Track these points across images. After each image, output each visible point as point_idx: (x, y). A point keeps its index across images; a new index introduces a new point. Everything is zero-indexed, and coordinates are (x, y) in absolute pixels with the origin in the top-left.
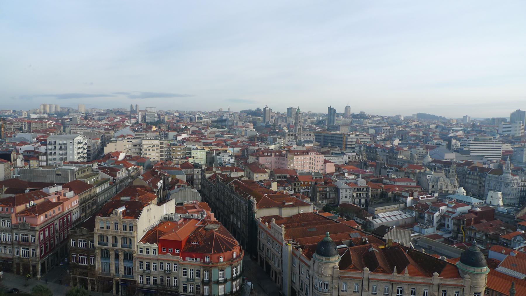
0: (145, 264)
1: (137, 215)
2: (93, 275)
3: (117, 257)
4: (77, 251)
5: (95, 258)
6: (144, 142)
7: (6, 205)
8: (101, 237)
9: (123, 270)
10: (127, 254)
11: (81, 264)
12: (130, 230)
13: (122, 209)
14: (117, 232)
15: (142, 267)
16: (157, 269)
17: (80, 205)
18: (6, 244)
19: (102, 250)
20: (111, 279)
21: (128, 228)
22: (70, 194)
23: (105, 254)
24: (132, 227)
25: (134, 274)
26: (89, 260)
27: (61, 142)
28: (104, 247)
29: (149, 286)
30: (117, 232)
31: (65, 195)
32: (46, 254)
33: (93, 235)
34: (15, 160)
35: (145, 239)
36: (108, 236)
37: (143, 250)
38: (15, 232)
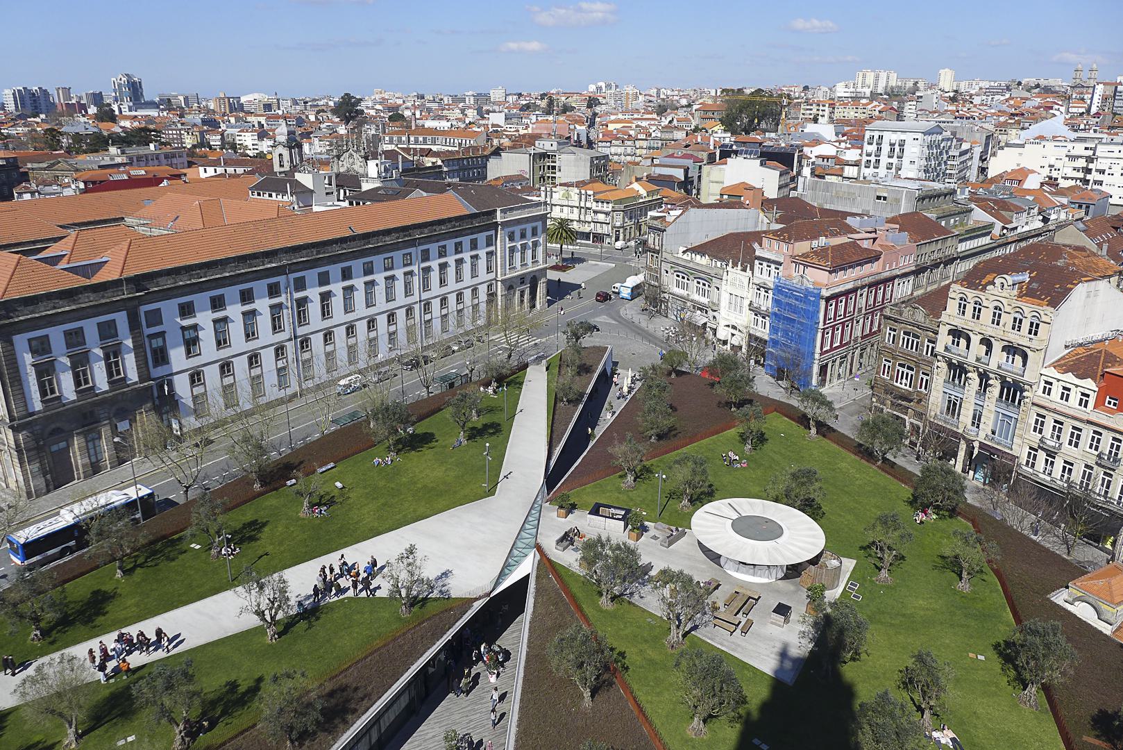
0: (1049, 423)
5: (932, 379)
11: (898, 384)
21: (1026, 326)
24: (1038, 325)
29: (1048, 479)
35: (1063, 366)
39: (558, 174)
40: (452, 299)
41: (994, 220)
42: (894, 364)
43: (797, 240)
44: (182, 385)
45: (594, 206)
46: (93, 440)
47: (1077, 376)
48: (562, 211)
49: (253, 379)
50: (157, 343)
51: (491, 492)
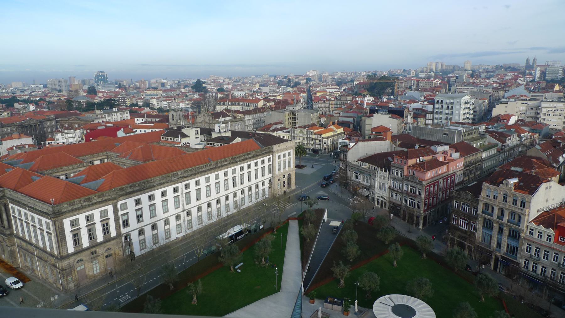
0: (534, 249)
1: (532, 191)
2: (472, 242)
3: (501, 231)
4: (458, 213)
5: (476, 225)
6: (544, 105)
7: (401, 157)
8: (486, 206)
9: (506, 247)
10: (513, 231)
12: (521, 206)
13: (514, 181)
14: (505, 205)
15: (529, 250)
16: (549, 259)
17: (465, 168)
18: (397, 191)
19: (485, 219)
20: (491, 252)
21: (519, 203)
22: (456, 155)
23: (488, 225)
24: (524, 203)
25: (518, 255)
26: (469, 225)
27: (448, 101)
28: (488, 217)
29: (535, 274)
30: (505, 205)
31: (451, 156)
32: (428, 209)
33: (477, 201)
34: (407, 117)
36: (494, 207)
37: (534, 232)
38: (405, 182)
39: (297, 121)
40: (253, 187)
41: (498, 142)
42: (458, 218)
43: (410, 159)
44: (135, 237)
45: (313, 136)
46: (96, 264)
47: (545, 227)
48: (299, 139)
49: (165, 230)
50: (125, 218)
51: (278, 290)
